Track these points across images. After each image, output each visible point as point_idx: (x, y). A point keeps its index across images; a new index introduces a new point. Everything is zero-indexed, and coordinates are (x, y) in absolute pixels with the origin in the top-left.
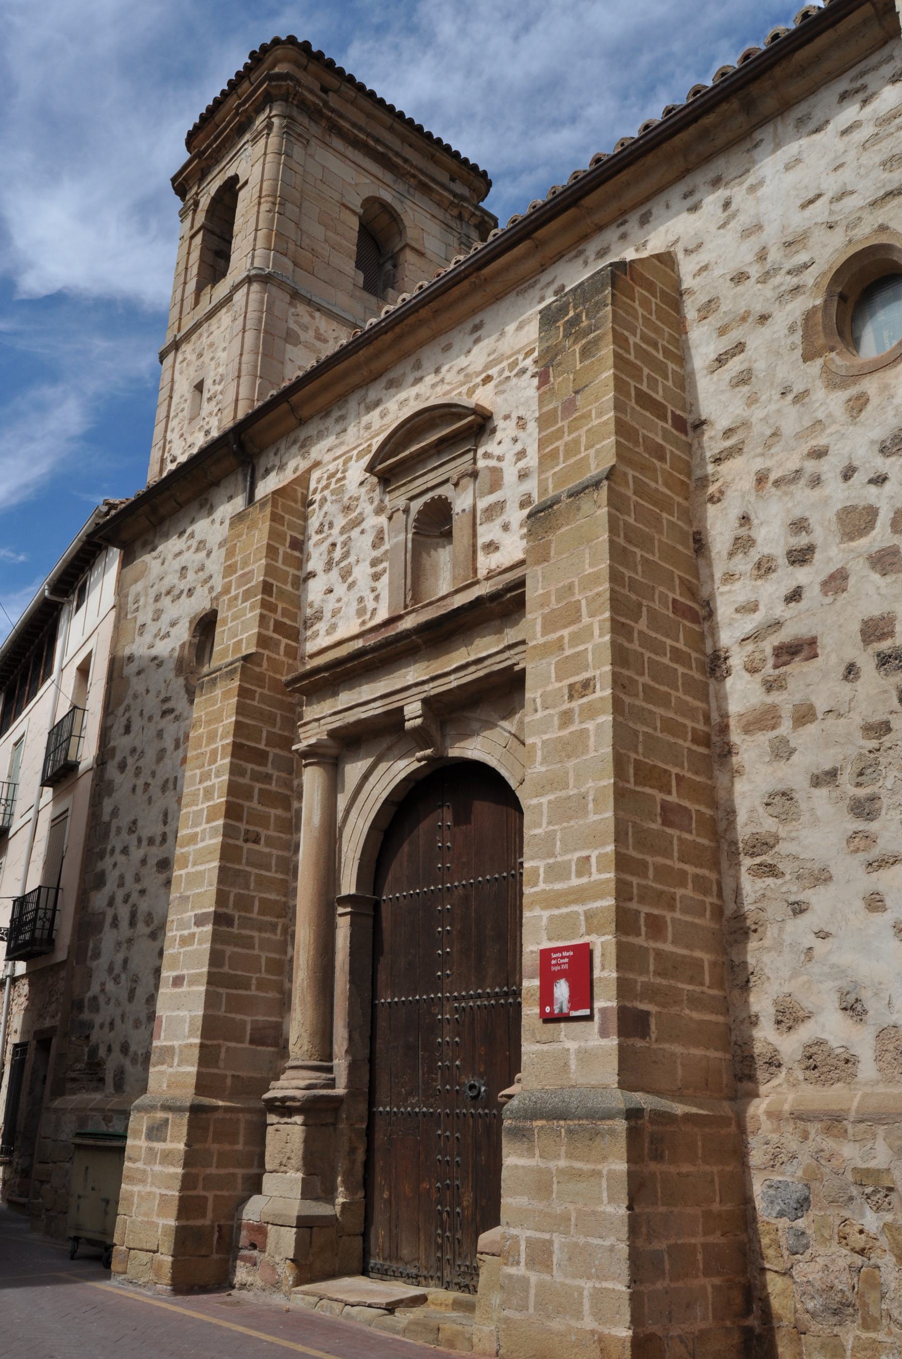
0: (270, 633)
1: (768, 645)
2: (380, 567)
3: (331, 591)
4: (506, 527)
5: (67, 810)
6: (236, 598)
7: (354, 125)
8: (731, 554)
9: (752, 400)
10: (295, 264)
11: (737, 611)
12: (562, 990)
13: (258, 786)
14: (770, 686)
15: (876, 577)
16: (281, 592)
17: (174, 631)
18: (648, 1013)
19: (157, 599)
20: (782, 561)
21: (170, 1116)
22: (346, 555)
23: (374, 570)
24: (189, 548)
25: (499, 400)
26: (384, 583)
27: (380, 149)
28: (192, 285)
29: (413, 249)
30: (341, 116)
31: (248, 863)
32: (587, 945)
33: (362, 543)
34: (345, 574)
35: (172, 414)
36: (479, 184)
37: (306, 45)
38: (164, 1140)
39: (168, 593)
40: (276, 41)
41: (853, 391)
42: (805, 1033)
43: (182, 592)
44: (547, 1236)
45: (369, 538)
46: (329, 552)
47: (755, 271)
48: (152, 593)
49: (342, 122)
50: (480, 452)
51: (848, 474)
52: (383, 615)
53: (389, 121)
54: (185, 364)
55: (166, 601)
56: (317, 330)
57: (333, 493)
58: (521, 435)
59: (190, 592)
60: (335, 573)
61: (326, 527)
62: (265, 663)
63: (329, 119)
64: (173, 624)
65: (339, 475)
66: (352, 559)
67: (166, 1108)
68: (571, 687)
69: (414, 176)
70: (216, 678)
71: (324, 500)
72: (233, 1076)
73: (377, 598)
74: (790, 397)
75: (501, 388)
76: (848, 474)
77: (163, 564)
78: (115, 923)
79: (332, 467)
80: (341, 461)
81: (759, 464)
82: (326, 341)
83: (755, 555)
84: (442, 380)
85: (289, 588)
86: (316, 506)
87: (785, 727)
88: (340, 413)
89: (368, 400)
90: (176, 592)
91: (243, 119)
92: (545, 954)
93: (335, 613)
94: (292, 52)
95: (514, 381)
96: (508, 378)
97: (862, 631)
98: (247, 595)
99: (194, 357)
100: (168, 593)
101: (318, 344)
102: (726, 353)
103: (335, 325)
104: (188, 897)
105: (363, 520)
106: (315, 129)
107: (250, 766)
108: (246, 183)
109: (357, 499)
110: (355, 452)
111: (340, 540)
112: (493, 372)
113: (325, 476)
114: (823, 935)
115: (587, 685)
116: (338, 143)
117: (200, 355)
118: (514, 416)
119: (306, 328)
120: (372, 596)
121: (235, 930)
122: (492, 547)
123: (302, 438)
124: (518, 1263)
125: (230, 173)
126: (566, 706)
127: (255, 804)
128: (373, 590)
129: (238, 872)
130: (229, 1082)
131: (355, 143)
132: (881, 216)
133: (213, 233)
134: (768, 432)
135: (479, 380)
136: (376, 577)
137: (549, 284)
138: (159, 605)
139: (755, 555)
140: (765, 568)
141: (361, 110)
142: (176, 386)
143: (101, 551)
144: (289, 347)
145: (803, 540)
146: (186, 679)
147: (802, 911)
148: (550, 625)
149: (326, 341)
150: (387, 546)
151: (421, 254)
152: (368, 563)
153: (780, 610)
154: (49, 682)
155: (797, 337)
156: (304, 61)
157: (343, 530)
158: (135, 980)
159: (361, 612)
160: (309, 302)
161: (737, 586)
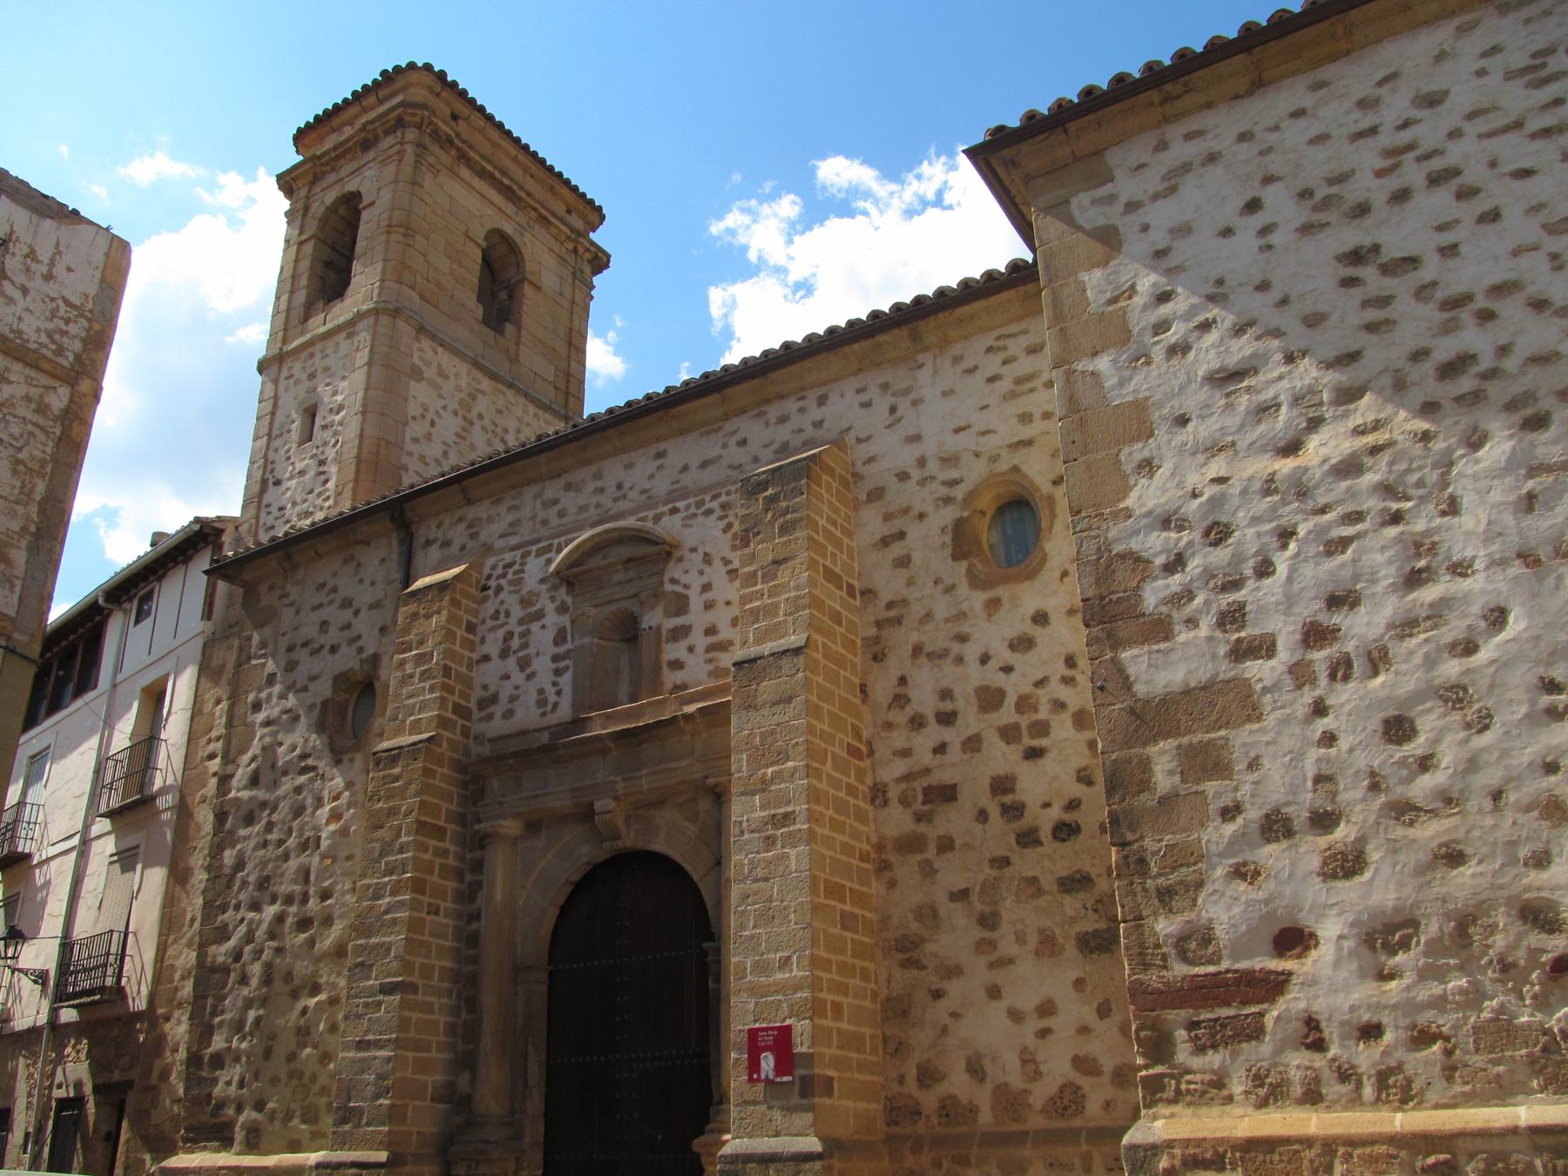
0: (449, 715)
1: (919, 785)
2: (563, 664)
4: (691, 649)
5: (137, 847)
7: (483, 157)
8: (890, 706)
9: (910, 582)
10: (422, 297)
11: (894, 754)
12: (768, 1062)
13: (438, 861)
14: (919, 818)
15: (1003, 745)
16: (458, 674)
17: (312, 687)
18: (831, 1079)
19: (290, 649)
20: (931, 719)
22: (525, 646)
24: (331, 602)
25: (686, 531)
26: (566, 680)
27: (506, 181)
28: (301, 296)
29: (531, 282)
30: (471, 148)
31: (431, 934)
32: (789, 1028)
33: (542, 638)
34: (524, 664)
35: (275, 432)
36: (593, 217)
37: (442, 75)
39: (305, 644)
40: (412, 66)
41: (990, 594)
42: (941, 1089)
43: (322, 647)
45: (551, 634)
46: (505, 640)
47: (915, 474)
48: (284, 642)
49: (472, 154)
50: (667, 577)
51: (985, 659)
52: (565, 712)
53: (513, 151)
54: (291, 381)
55: (302, 655)
56: (439, 366)
57: (510, 583)
58: (707, 569)
59: (334, 649)
60: (511, 663)
61: (502, 615)
62: (445, 745)
63: (458, 149)
64: (313, 679)
65: (517, 567)
66: (531, 650)
69: (535, 210)
71: (499, 589)
72: (419, 1133)
73: (559, 693)
74: (941, 587)
76: (985, 659)
77: (298, 612)
78: (244, 980)
79: (508, 557)
80: (519, 553)
81: (915, 637)
82: (447, 377)
83: (909, 711)
84: (624, 496)
85: (464, 670)
86: (491, 592)
87: (931, 852)
88: (512, 503)
90: (316, 646)
91: (370, 136)
92: (753, 1033)
93: (513, 699)
94: (428, 79)
95: (701, 519)
96: (695, 515)
97: (992, 787)
98: (424, 676)
99: (304, 376)
100: (305, 644)
101: (439, 380)
102: (891, 536)
103: (456, 361)
105: (543, 616)
106: (446, 158)
107: (432, 843)
108: (372, 204)
110: (534, 548)
111: (518, 630)
112: (681, 505)
113: (501, 564)
115: (788, 818)
116: (465, 172)
117: (312, 376)
118: (701, 550)
119: (428, 364)
120: (553, 690)
121: (420, 997)
122: (677, 665)
123: (470, 517)
125: (351, 187)
127: (435, 878)
128: (555, 684)
129: (422, 943)
130: (414, 1136)
131: (482, 174)
132: (1015, 459)
133: (324, 242)
134: (923, 612)
135: (666, 509)
136: (558, 673)
138: (293, 656)
139: (909, 711)
140: (917, 723)
141: (488, 139)
142: (280, 403)
143: (176, 564)
144: (413, 383)
145: (948, 706)
146: (330, 737)
148: (757, 761)
149: (447, 377)
150: (569, 646)
151: (538, 288)
152: (548, 658)
153: (927, 758)
154: (90, 695)
155: (948, 539)
156: (438, 88)
157: (521, 622)
158: (272, 1037)
159: (542, 702)
160: (433, 337)
161: (895, 734)
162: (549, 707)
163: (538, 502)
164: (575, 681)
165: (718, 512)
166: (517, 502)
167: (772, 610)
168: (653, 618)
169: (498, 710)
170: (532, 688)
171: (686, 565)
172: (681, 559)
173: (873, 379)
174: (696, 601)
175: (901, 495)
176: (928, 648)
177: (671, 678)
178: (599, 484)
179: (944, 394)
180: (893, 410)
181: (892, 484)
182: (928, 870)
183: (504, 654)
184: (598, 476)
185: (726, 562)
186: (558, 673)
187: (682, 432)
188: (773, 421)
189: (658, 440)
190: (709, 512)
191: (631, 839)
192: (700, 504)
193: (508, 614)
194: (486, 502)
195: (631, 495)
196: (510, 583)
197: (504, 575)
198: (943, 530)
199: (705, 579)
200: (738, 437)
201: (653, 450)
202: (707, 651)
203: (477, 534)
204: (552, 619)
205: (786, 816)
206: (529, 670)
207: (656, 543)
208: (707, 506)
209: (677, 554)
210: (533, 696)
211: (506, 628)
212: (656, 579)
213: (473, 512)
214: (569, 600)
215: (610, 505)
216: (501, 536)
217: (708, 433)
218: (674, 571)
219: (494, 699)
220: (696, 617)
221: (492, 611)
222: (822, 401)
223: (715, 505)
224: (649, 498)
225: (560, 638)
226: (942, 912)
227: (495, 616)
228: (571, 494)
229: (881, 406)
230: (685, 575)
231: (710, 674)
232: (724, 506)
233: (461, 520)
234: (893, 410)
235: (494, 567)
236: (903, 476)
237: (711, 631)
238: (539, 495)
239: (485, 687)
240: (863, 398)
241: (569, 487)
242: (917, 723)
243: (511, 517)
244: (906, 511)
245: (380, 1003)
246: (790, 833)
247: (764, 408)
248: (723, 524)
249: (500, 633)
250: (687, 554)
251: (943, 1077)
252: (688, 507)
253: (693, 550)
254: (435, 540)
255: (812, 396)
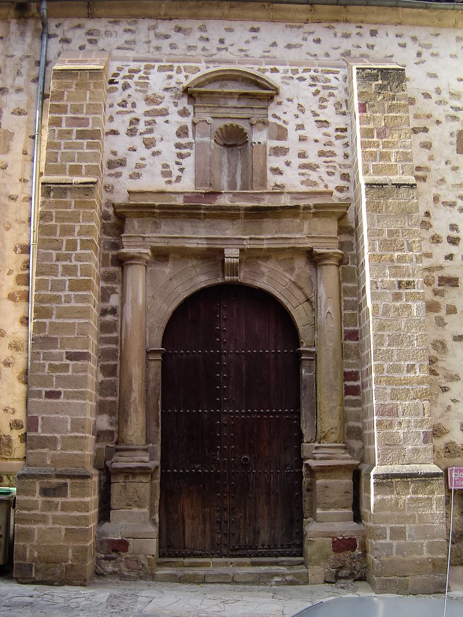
1: (436, 275)
2: (184, 151)
3: (135, 151)
6: (69, 132)
9: (431, 158)
14: (436, 293)
21: (68, 481)
23: (178, 151)
38: (65, 496)
42: (446, 439)
44: (403, 526)
46: (131, 123)
47: (435, 97)
50: (270, 113)
57: (137, 84)
61: (129, 105)
65: (141, 74)
67: (59, 476)
68: (400, 283)
70: (65, 189)
71: (126, 87)
73: (182, 170)
74: (449, 166)
75: (286, 81)
80: (143, 64)
81: (434, 191)
83: (431, 232)
87: (443, 313)
89: (158, 31)
93: (138, 166)
95: (297, 82)
104: (56, 339)
109: (163, 98)
110: (157, 65)
113: (127, 69)
114: (454, 401)
118: (296, 101)
124: (386, 538)
126: (397, 291)
134: (440, 178)
137: (310, 33)
139: (431, 232)
140: (436, 239)
145: (454, 234)
147: (446, 391)
150: (190, 139)
152: (172, 144)
153: (442, 261)
155: (454, 139)
162: (174, 179)
163: (152, 32)
164: (197, 165)
165: (309, 81)
166: (132, 27)
167: (384, 156)
168: (258, 137)
169: (126, 171)
170: (158, 162)
171: (283, 108)
172: (280, 103)
173: (409, 32)
174: (293, 135)
175: (423, 106)
176: (442, 199)
177: (272, 179)
178: (205, 35)
179: (451, 56)
180: (419, 54)
181: (420, 99)
182: (441, 323)
183: (132, 132)
184: (203, 29)
185: (315, 115)
186: (180, 156)
187: (273, 20)
188: (339, 35)
189: (254, 20)
190: (302, 79)
191: (243, 277)
192: (295, 72)
193: (134, 105)
194: (104, 21)
195: (231, 49)
196: (137, 84)
197: (131, 77)
198: (451, 134)
199: (299, 122)
200: (315, 36)
201: (250, 24)
202: (299, 167)
203: (96, 41)
204: (176, 120)
205: (408, 283)
206: (154, 149)
207: (266, 88)
208: (300, 75)
209: (277, 99)
210: (159, 169)
211: (133, 115)
212: (263, 112)
213: (90, 24)
214: (190, 108)
215: (214, 51)
216: (119, 48)
217: (292, 27)
218: (273, 109)
219: (122, 163)
220: (292, 141)
221: (120, 100)
222: (373, 33)
223: (306, 75)
224: (247, 56)
225: (182, 132)
226: (449, 346)
227: (123, 104)
228: (180, 35)
229: (413, 49)
230: (283, 113)
231: (302, 183)
232: (313, 78)
233: (79, 26)
234: (419, 54)
235: (120, 69)
236: (427, 96)
237: (302, 155)
238: (154, 28)
239: (114, 153)
240: (401, 41)
241: (179, 30)
242: (436, 239)
243: (128, 37)
244: (429, 117)
245: (68, 365)
246: (412, 294)
247: (333, 24)
248: (313, 89)
249: (128, 118)
250: (285, 102)
251: (448, 432)
252: (286, 71)
253: (289, 100)
254: (55, 36)
255: (366, 29)
